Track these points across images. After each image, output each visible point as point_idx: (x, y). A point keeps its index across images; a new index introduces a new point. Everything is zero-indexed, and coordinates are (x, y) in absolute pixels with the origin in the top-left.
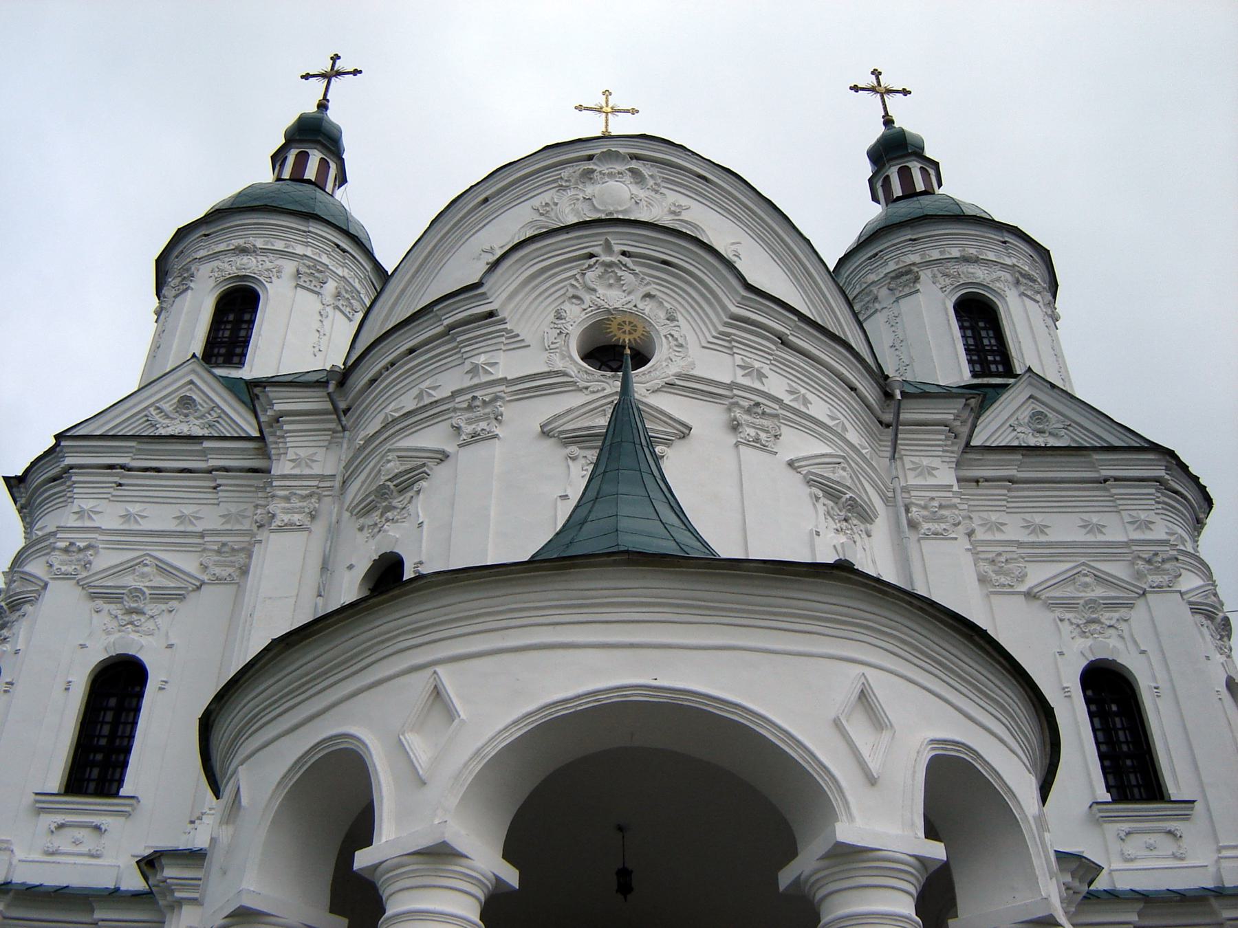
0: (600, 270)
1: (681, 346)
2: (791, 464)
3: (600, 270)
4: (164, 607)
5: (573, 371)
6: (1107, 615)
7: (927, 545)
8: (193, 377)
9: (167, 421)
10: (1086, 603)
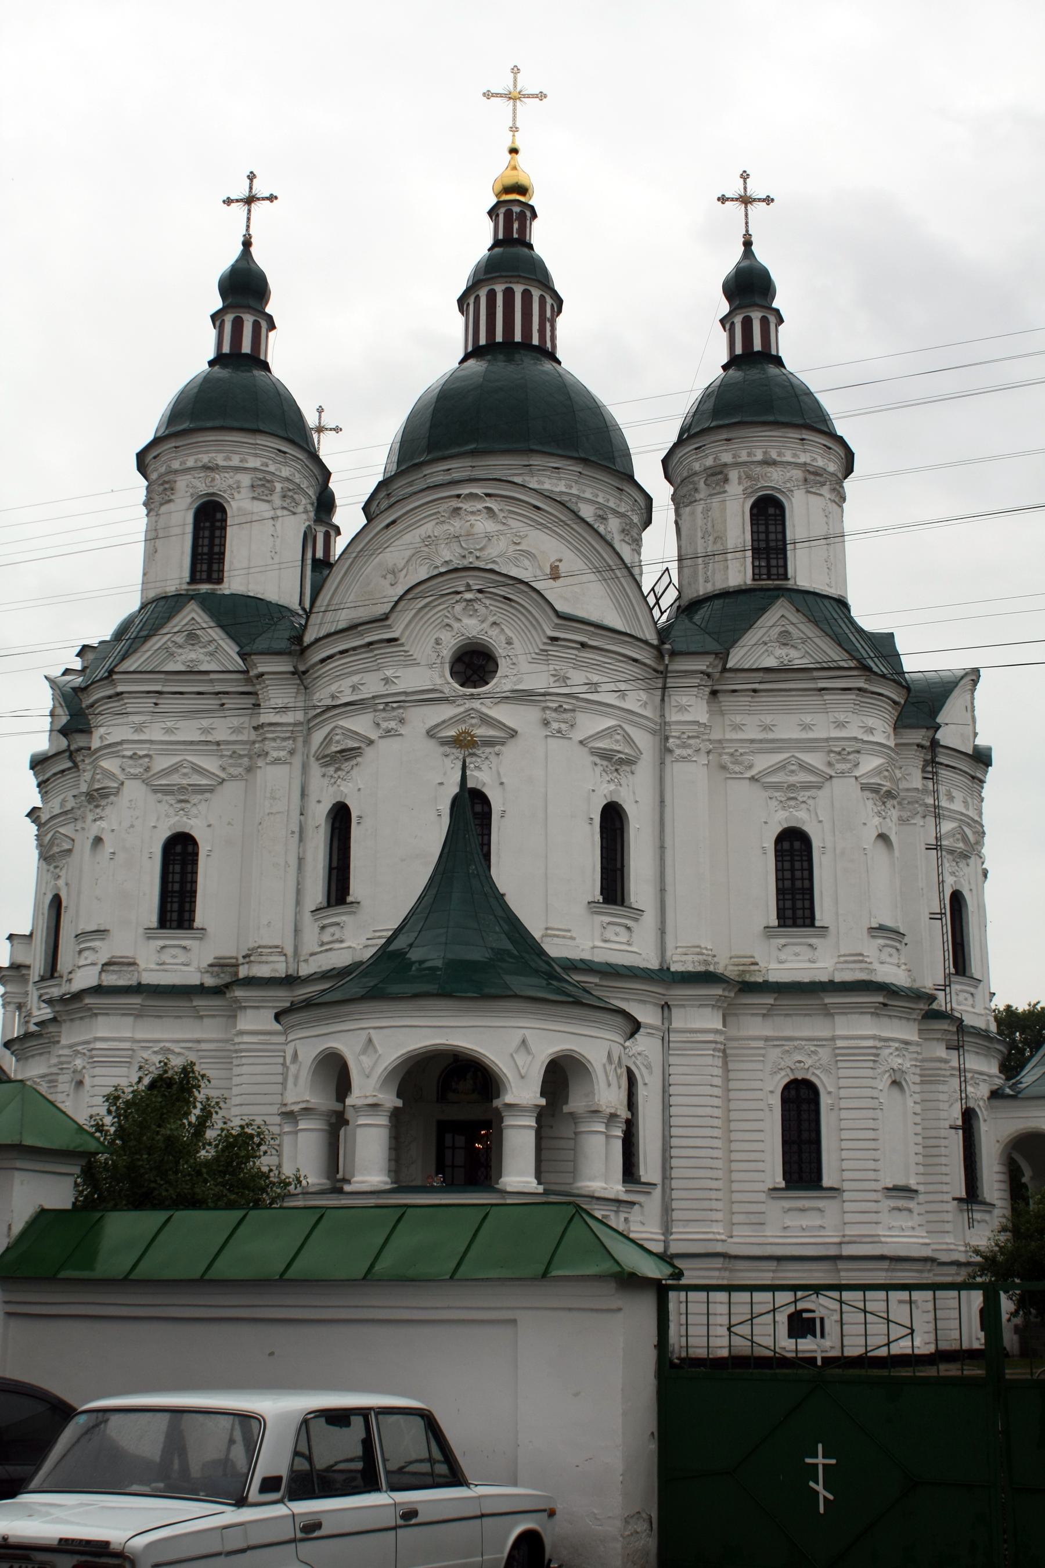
0: (464, 604)
1: (514, 664)
2: (581, 742)
3: (464, 604)
4: (200, 797)
5: (446, 691)
6: (802, 793)
7: (677, 766)
8: (193, 615)
9: (180, 651)
10: (789, 786)
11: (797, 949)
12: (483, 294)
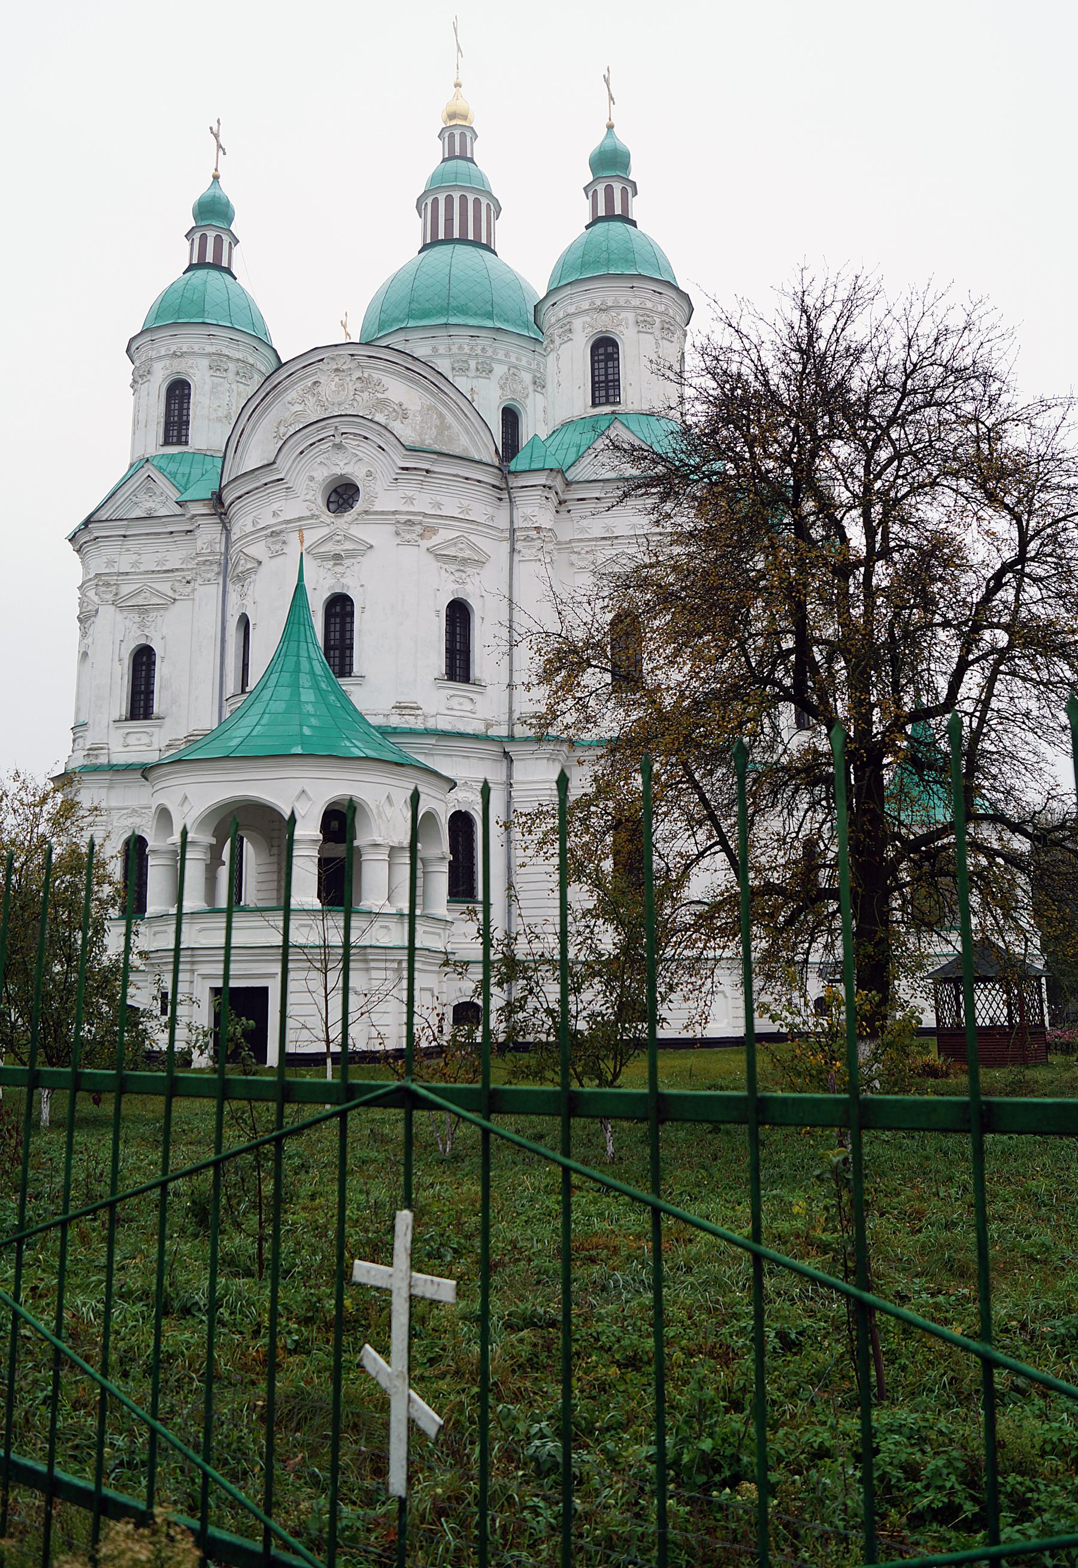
12: (429, 201)
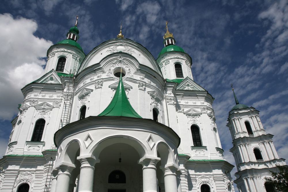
11: (199, 152)
